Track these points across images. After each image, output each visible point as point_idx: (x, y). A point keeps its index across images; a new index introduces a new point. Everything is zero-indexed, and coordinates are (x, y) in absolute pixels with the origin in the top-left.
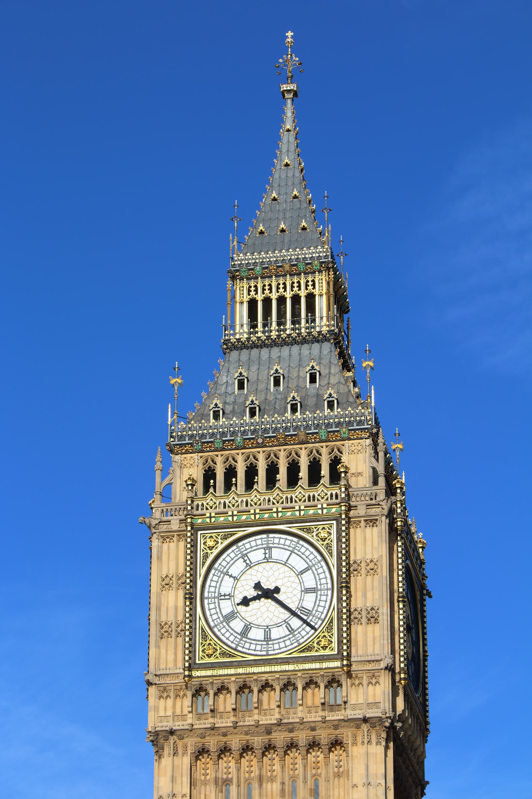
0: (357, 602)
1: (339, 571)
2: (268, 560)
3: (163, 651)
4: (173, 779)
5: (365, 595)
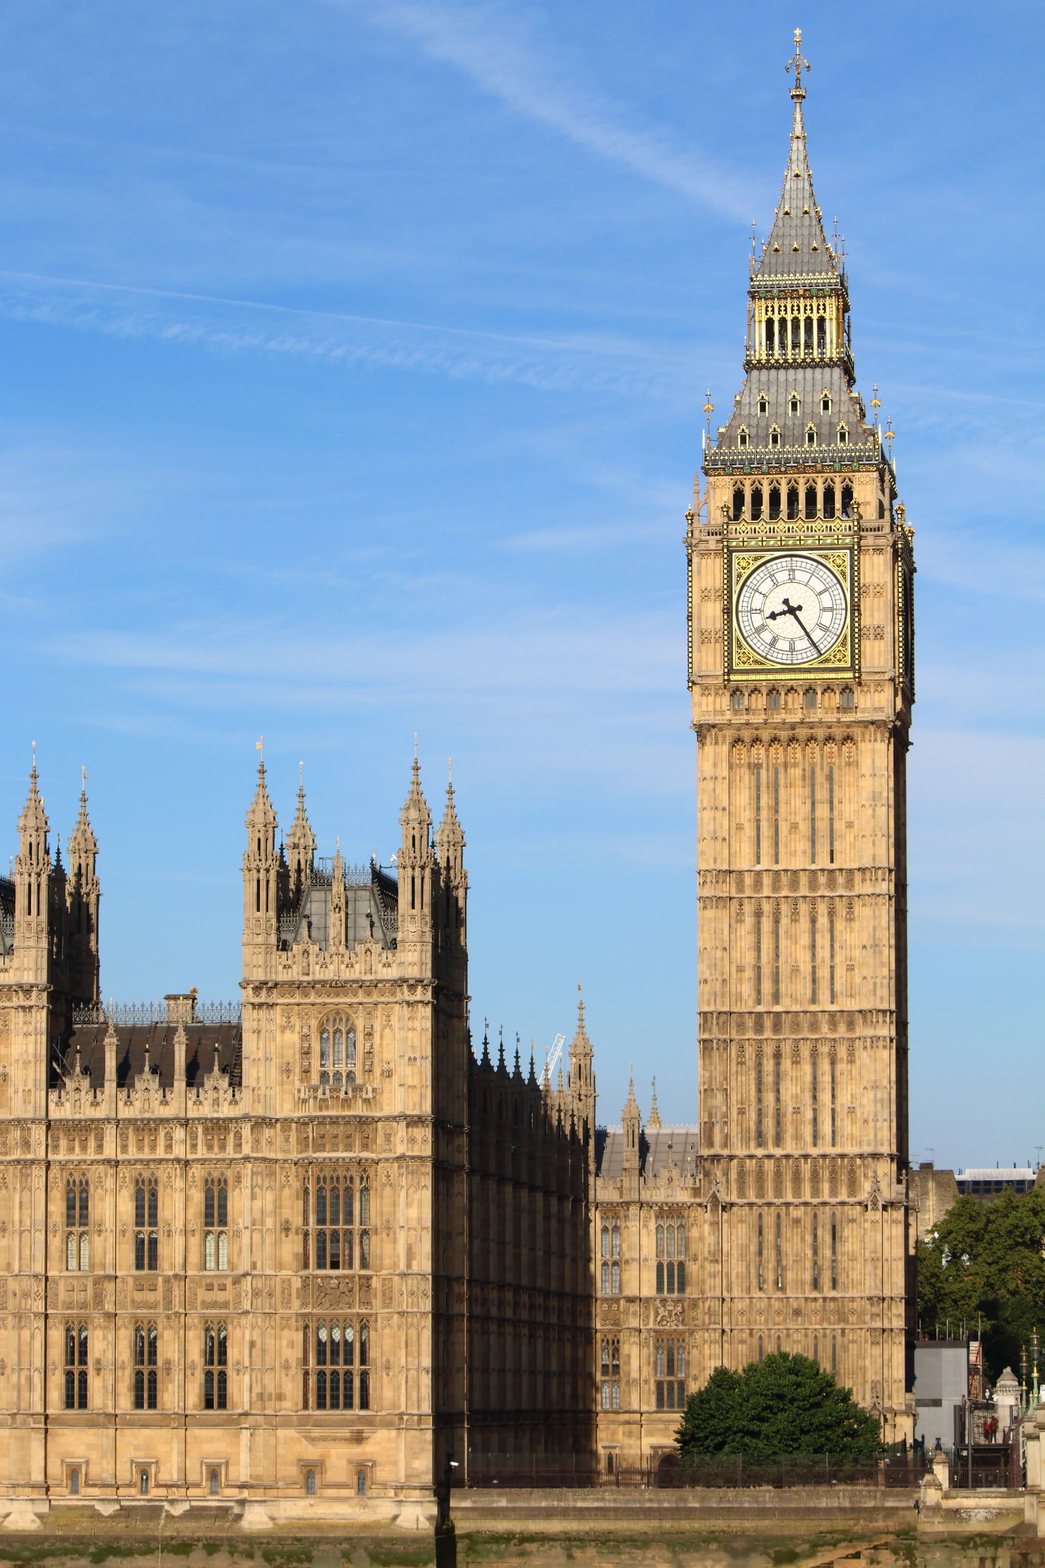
0: (866, 620)
1: (852, 595)
2: (792, 580)
3: (704, 654)
4: (715, 765)
5: (872, 615)
